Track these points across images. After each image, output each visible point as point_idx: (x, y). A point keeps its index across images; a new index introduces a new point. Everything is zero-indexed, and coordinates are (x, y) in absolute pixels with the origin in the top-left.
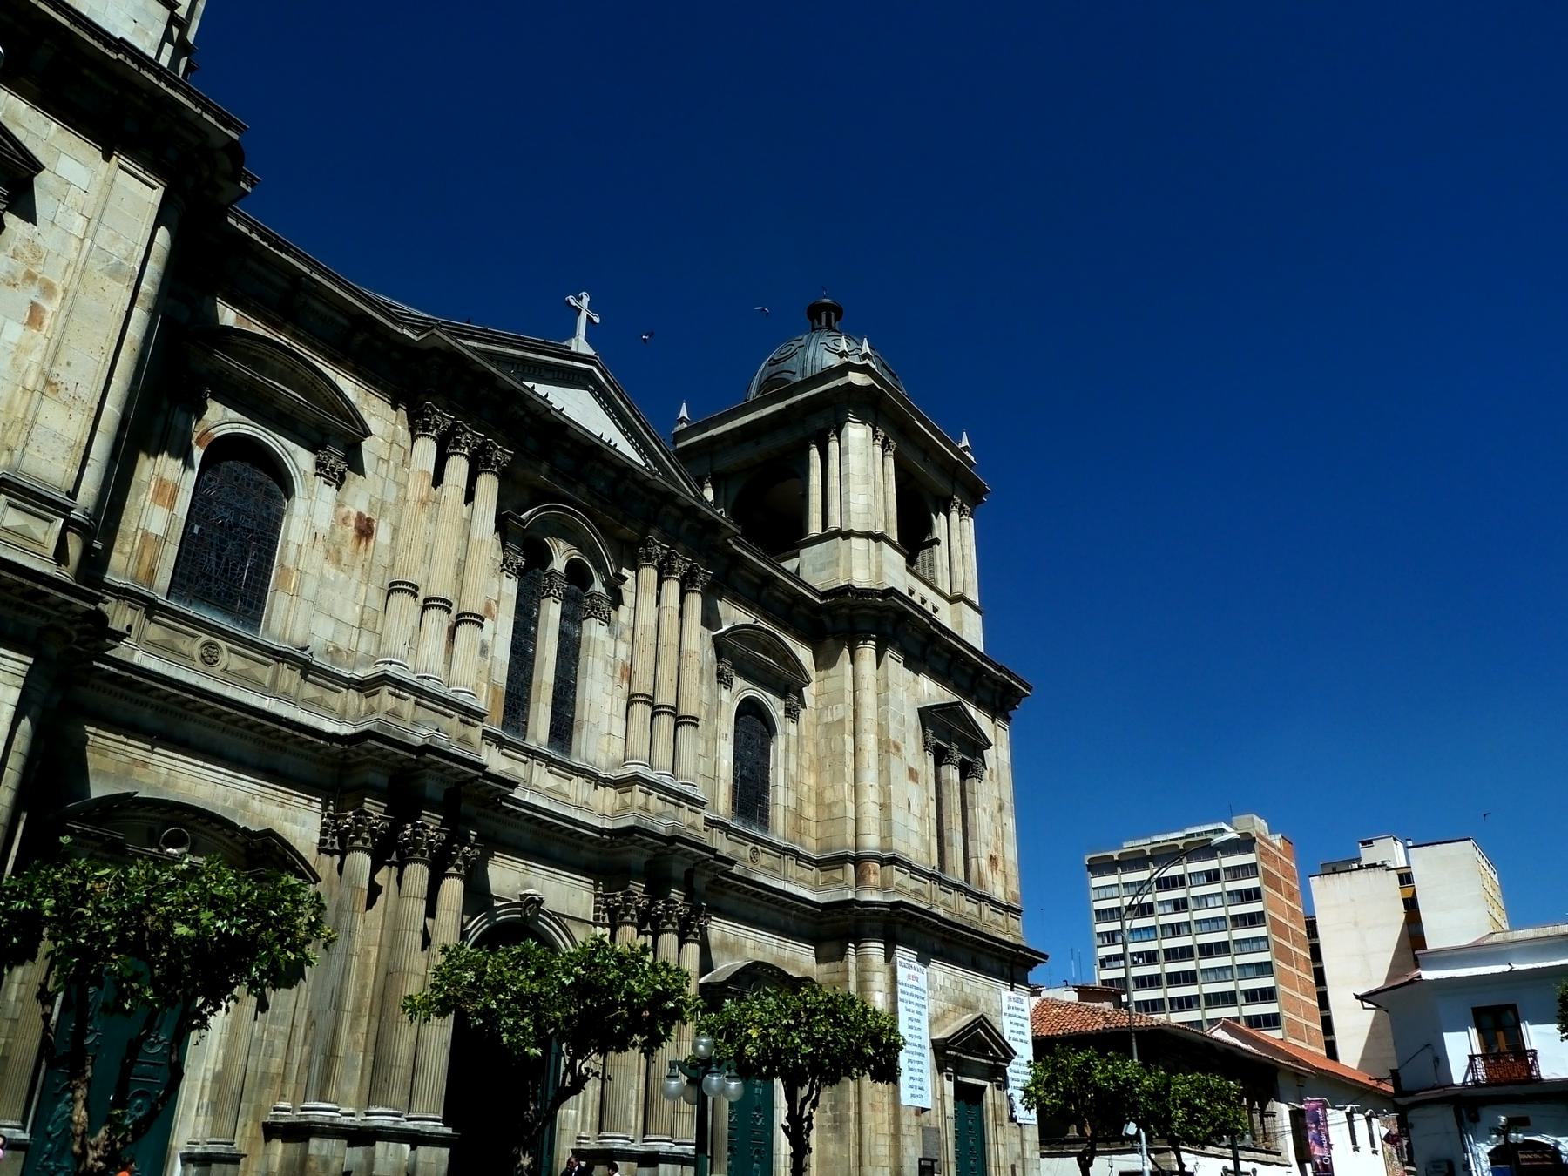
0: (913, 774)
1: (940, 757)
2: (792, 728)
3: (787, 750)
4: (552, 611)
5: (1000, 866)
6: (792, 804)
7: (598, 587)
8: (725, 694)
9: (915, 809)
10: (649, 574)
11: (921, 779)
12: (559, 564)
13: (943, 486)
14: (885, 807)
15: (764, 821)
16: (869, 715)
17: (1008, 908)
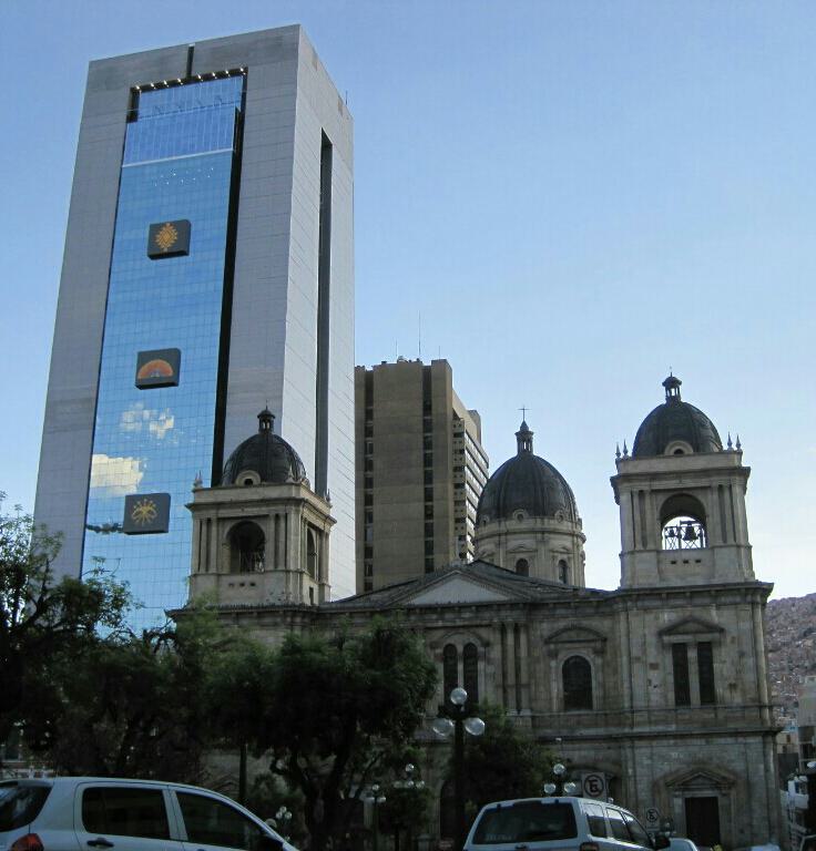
0: (654, 666)
1: (679, 651)
2: (599, 661)
3: (597, 672)
4: (460, 667)
5: (740, 686)
6: (601, 694)
7: (481, 649)
8: (553, 663)
9: (655, 683)
10: (498, 636)
11: (661, 667)
12: (460, 649)
13: (703, 482)
14: (631, 688)
15: (590, 706)
16: (624, 648)
17: (744, 707)
